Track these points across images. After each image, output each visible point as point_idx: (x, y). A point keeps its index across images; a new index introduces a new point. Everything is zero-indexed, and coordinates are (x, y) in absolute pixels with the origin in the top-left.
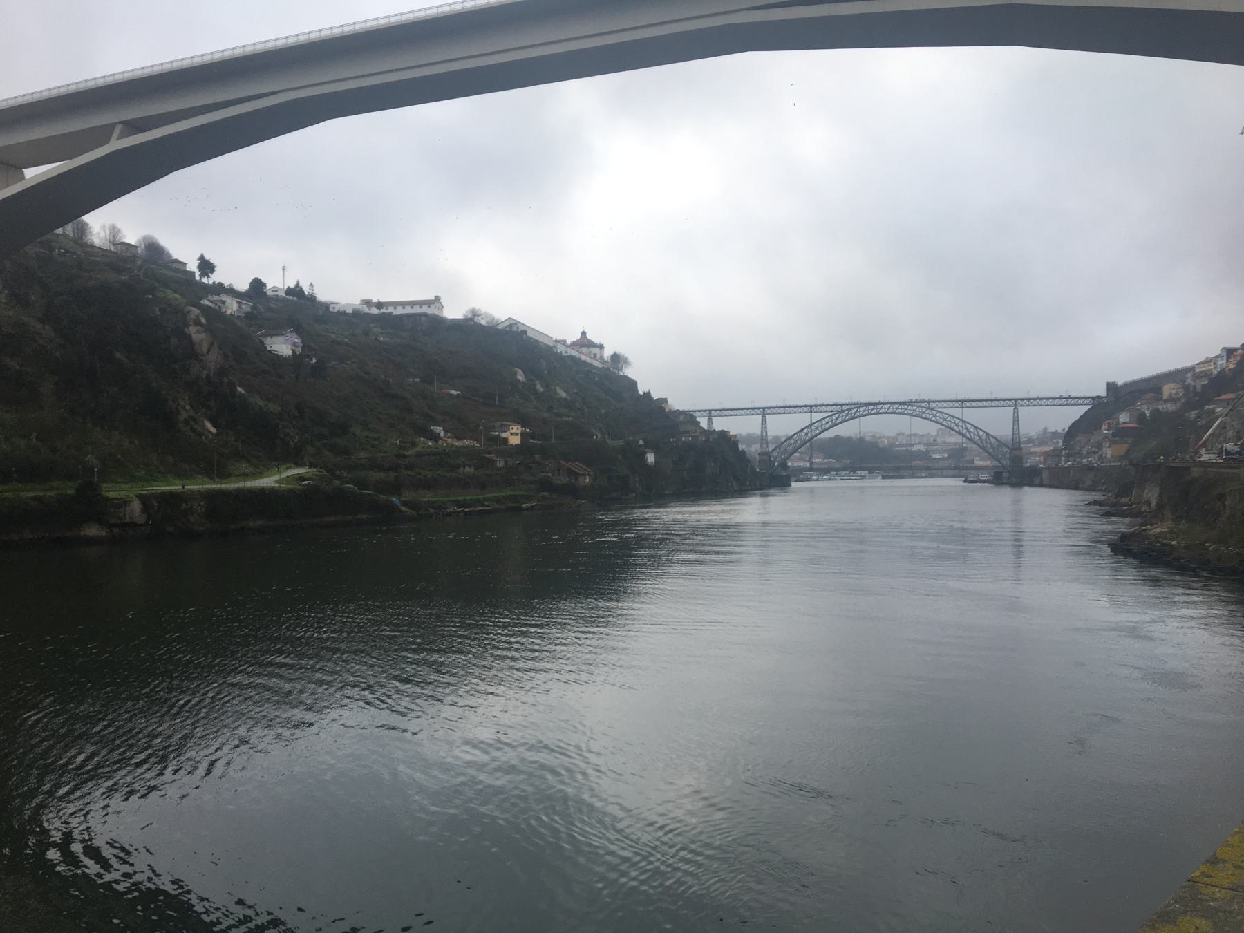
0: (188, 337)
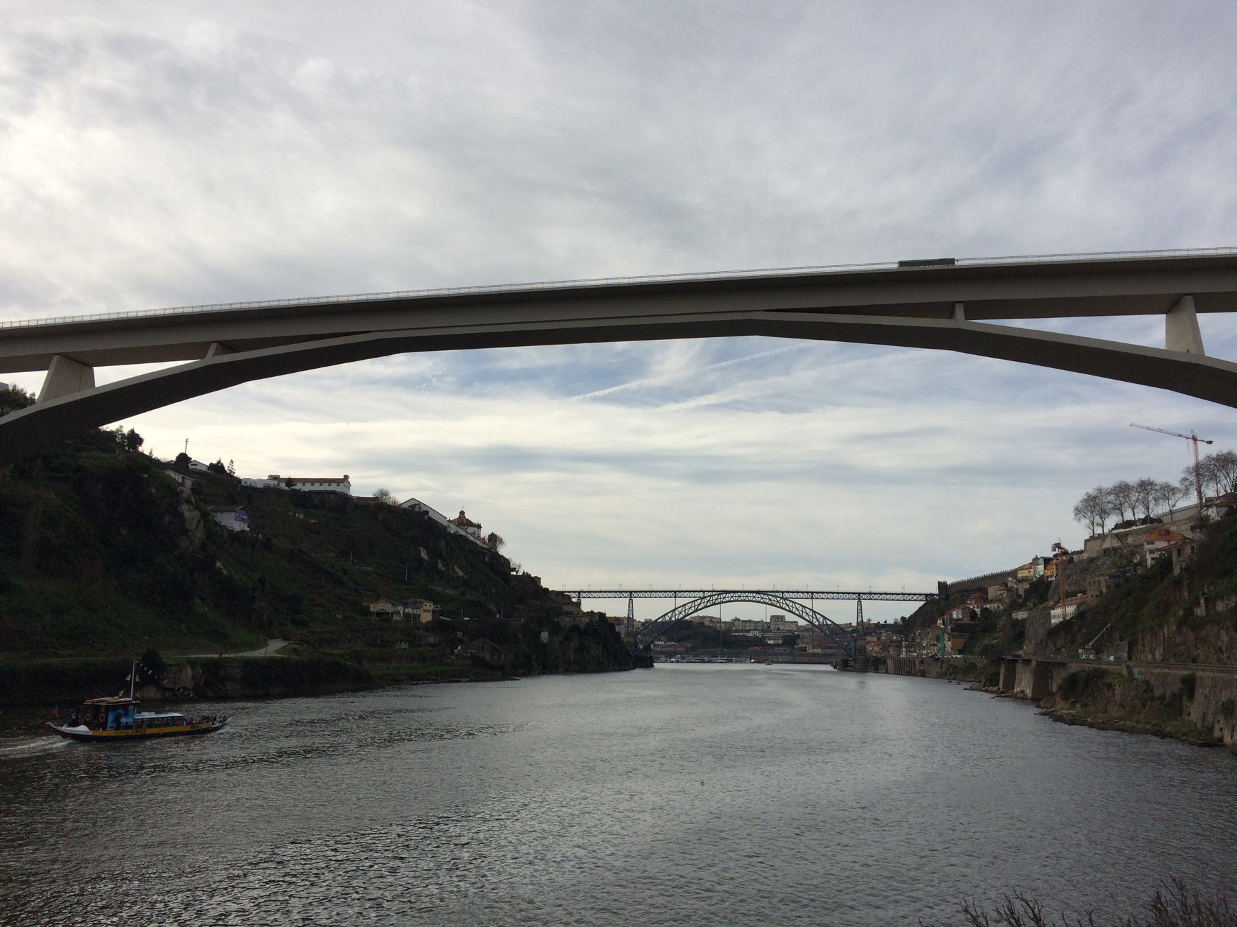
0: (180, 515)
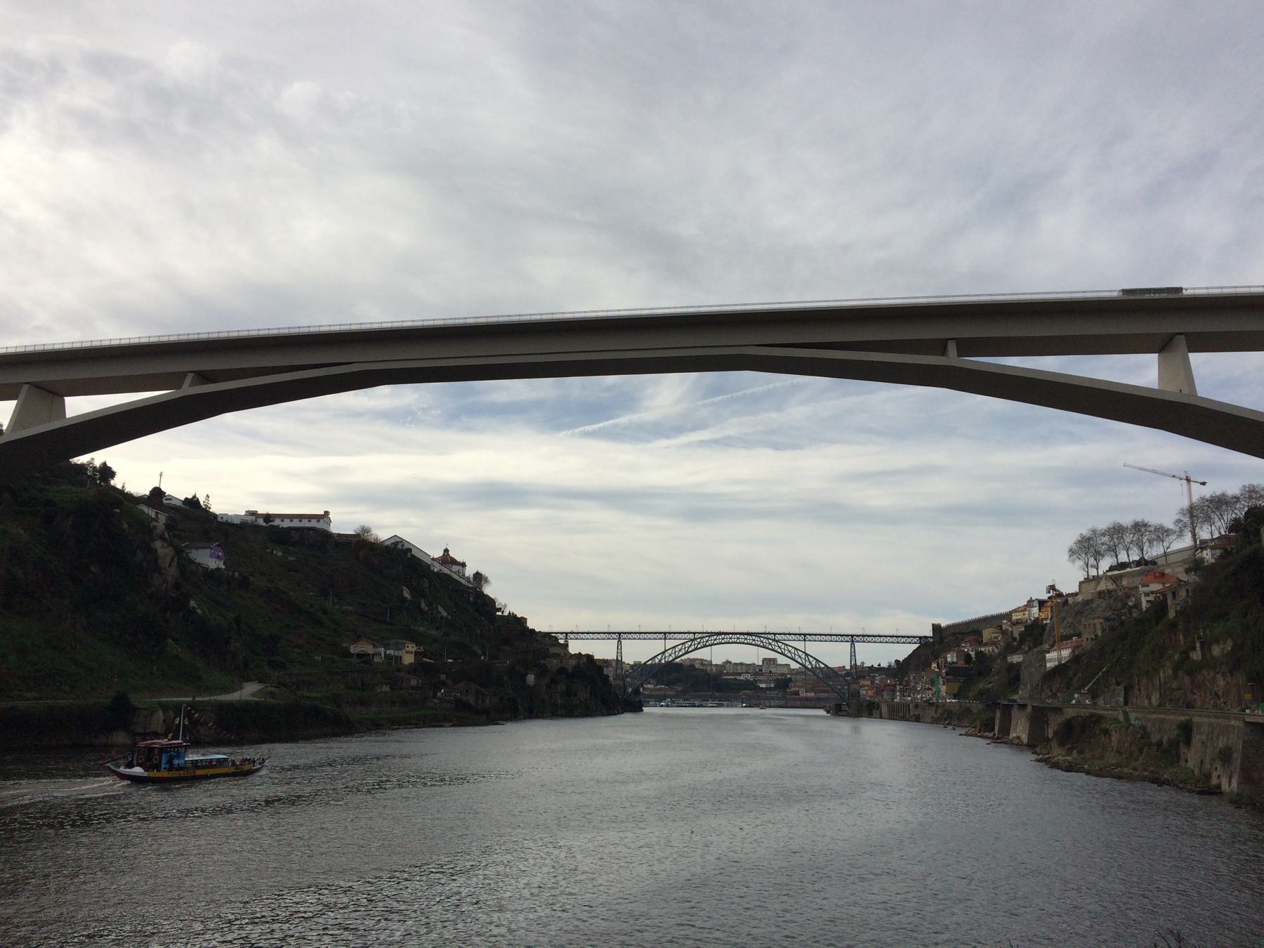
0: (153, 551)
